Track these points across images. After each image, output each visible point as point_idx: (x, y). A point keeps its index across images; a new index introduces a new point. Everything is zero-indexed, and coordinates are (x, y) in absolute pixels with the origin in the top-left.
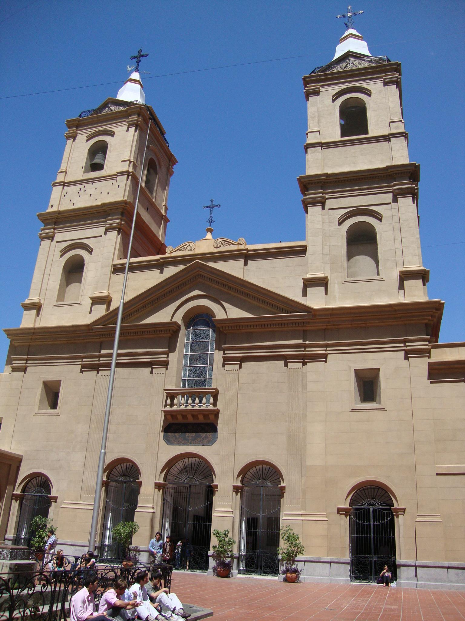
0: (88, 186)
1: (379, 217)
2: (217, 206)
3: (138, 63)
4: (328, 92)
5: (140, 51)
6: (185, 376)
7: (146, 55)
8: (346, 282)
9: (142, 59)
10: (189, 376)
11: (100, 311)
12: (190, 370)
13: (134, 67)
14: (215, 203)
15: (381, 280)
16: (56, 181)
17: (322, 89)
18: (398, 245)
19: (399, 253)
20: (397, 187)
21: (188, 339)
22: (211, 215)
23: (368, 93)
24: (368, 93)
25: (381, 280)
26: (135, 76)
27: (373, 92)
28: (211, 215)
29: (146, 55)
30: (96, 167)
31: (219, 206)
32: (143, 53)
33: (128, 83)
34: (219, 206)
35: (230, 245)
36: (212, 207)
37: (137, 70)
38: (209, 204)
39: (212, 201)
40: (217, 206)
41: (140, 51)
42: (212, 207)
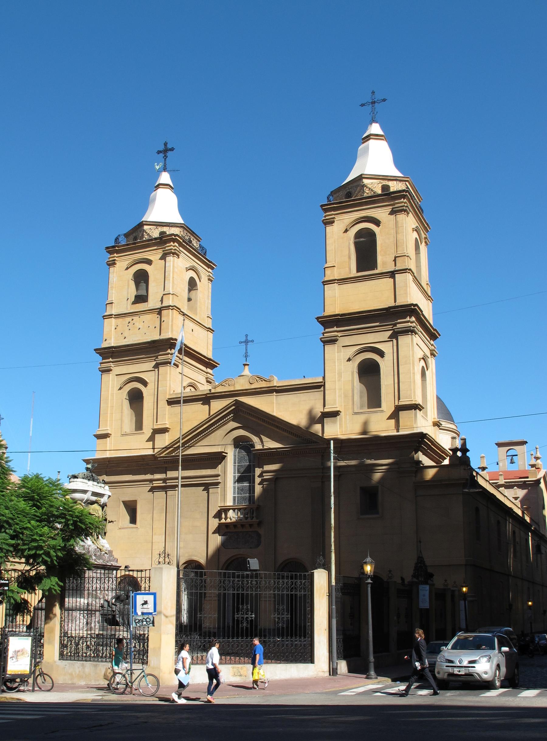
0: (136, 318)
3: (165, 159)
4: (343, 220)
5: (166, 144)
6: (234, 493)
7: (172, 149)
9: (169, 154)
10: (238, 494)
11: (163, 441)
12: (238, 488)
13: (161, 164)
15: (382, 411)
16: (106, 314)
17: (337, 218)
21: (235, 463)
22: (246, 350)
23: (377, 223)
24: (377, 223)
25: (382, 411)
26: (165, 178)
28: (246, 350)
29: (172, 149)
30: (141, 299)
32: (169, 146)
33: (160, 191)
36: (246, 342)
37: (165, 169)
41: (166, 144)
42: (246, 342)
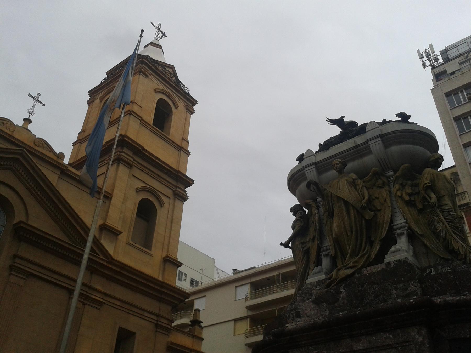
1: (161, 204)
2: (41, 103)
8: (129, 244)
14: (41, 99)
18: (167, 234)
19: (167, 240)
20: (178, 189)
23: (176, 107)
25: (151, 255)
27: (179, 108)
31: (44, 105)
34: (44, 105)
35: (50, 152)
38: (35, 95)
39: (39, 94)
40: (41, 103)
